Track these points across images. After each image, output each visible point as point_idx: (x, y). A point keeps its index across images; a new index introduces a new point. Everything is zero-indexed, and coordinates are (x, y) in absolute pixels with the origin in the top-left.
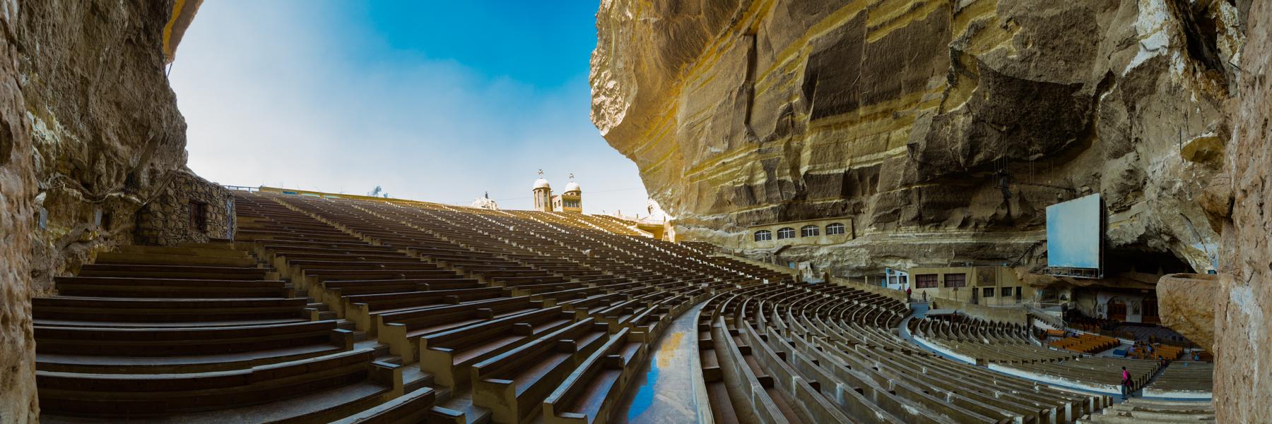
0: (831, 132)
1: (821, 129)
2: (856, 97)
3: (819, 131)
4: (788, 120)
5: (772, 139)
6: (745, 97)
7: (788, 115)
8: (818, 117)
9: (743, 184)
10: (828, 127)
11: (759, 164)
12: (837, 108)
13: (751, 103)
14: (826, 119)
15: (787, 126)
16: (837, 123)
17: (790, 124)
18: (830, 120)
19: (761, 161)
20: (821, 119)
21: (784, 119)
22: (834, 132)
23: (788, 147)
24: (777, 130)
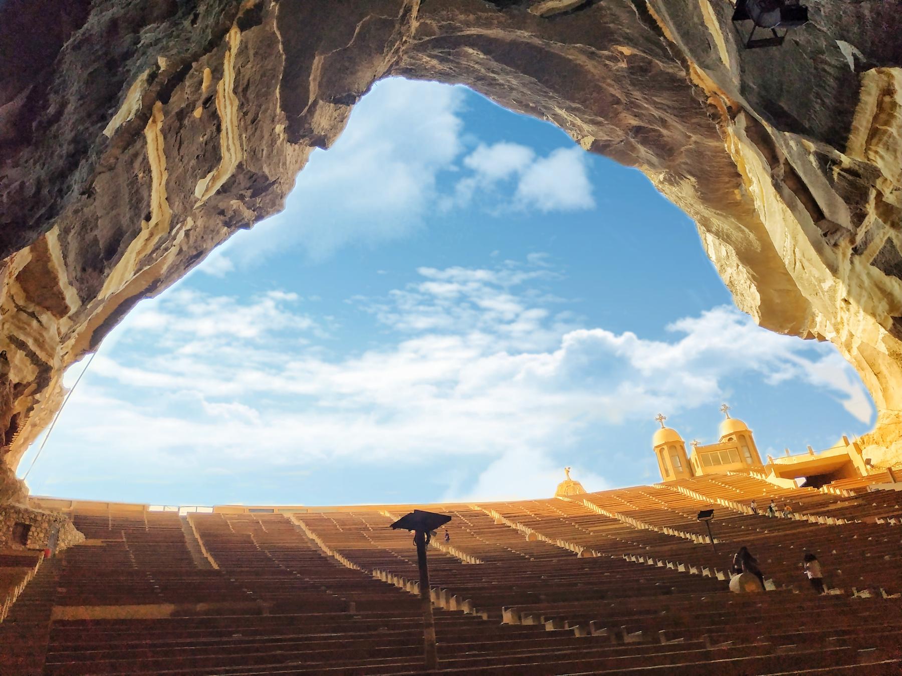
0: (891, 136)
1: (873, 148)
2: (833, 62)
3: (876, 152)
4: (839, 174)
5: (859, 218)
6: (787, 191)
7: (832, 170)
8: (846, 139)
9: (891, 321)
10: (874, 134)
11: (876, 272)
12: (841, 102)
13: (801, 189)
14: (857, 129)
15: (851, 183)
16: (876, 118)
17: (850, 178)
18: (863, 122)
19: (872, 264)
20: (851, 136)
21: (835, 177)
22: (893, 130)
23: (886, 211)
24: (847, 200)
